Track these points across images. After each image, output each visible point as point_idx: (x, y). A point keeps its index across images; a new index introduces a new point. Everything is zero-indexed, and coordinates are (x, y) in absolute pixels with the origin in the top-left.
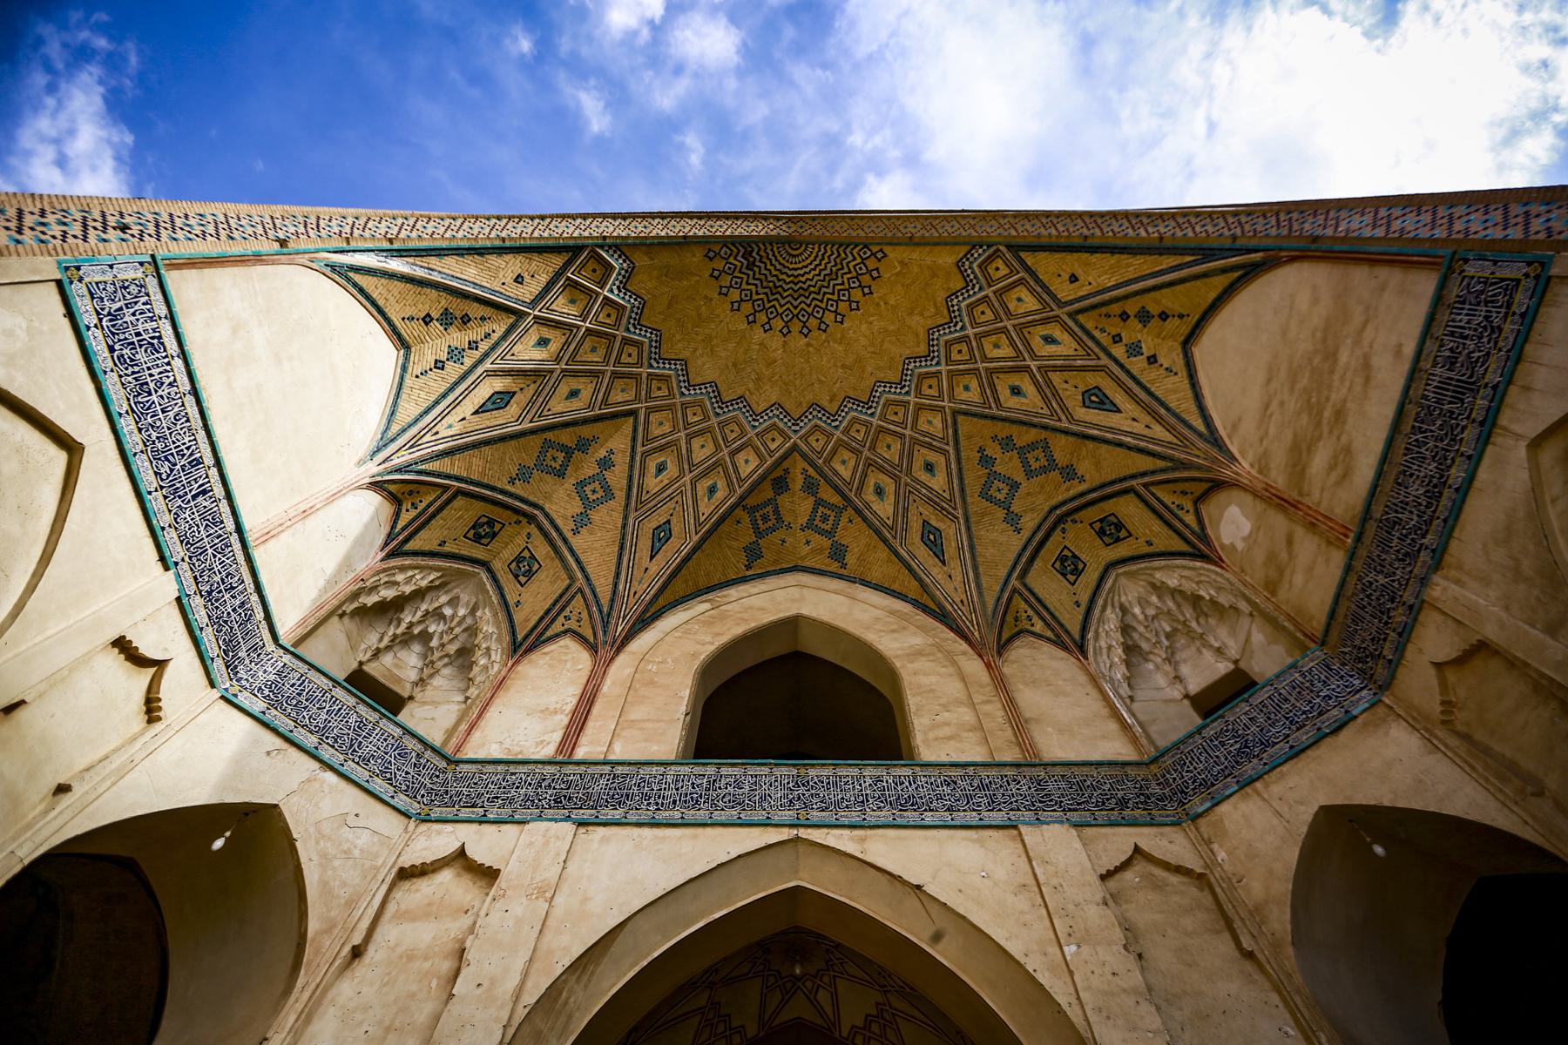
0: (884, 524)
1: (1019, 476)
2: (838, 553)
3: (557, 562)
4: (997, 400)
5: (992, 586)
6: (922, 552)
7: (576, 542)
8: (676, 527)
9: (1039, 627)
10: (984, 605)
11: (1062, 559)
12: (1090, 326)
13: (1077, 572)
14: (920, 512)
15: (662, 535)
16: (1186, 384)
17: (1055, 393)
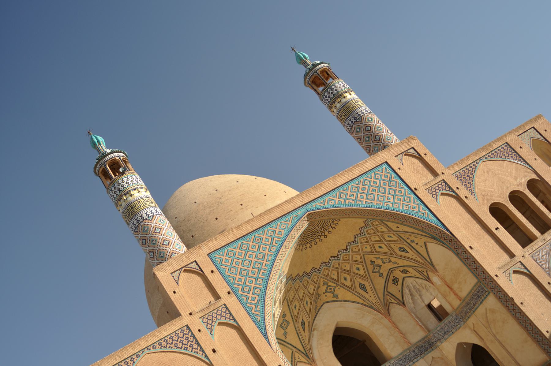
0: (350, 288)
1: (381, 263)
2: (336, 296)
3: (286, 348)
4: (375, 250)
5: (381, 296)
6: (361, 291)
7: (287, 340)
8: (305, 320)
9: (393, 301)
10: (381, 302)
11: (394, 280)
12: (401, 235)
13: (397, 282)
14: (358, 280)
16: (425, 250)
17: (392, 248)
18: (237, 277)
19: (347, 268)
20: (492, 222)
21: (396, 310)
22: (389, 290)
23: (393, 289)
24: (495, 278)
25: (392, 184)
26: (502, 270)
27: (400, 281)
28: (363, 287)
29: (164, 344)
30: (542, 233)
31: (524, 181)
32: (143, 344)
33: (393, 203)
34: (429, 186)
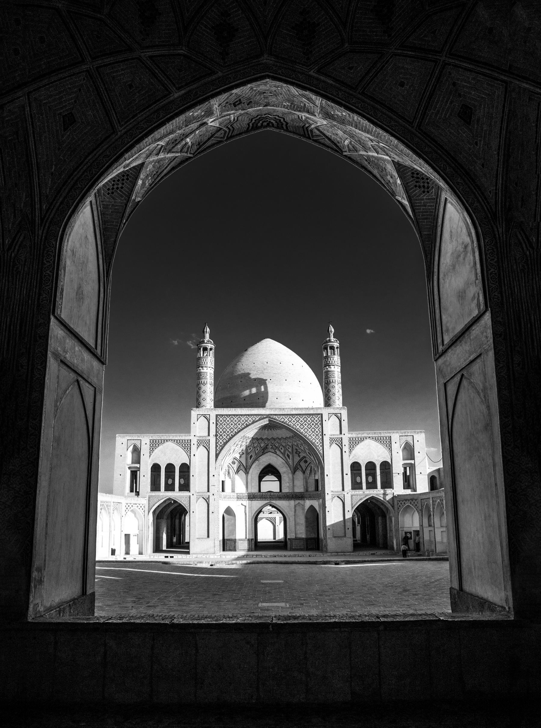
6: (287, 457)
15: (251, 457)
18: (221, 430)
19: (284, 445)
20: (347, 470)
21: (299, 474)
22: (301, 463)
23: (302, 464)
24: (326, 494)
25: (317, 426)
26: (332, 493)
27: (308, 463)
28: (288, 456)
29: (178, 442)
30: (367, 488)
31: (382, 460)
32: (171, 438)
33: (310, 435)
34: (333, 436)
